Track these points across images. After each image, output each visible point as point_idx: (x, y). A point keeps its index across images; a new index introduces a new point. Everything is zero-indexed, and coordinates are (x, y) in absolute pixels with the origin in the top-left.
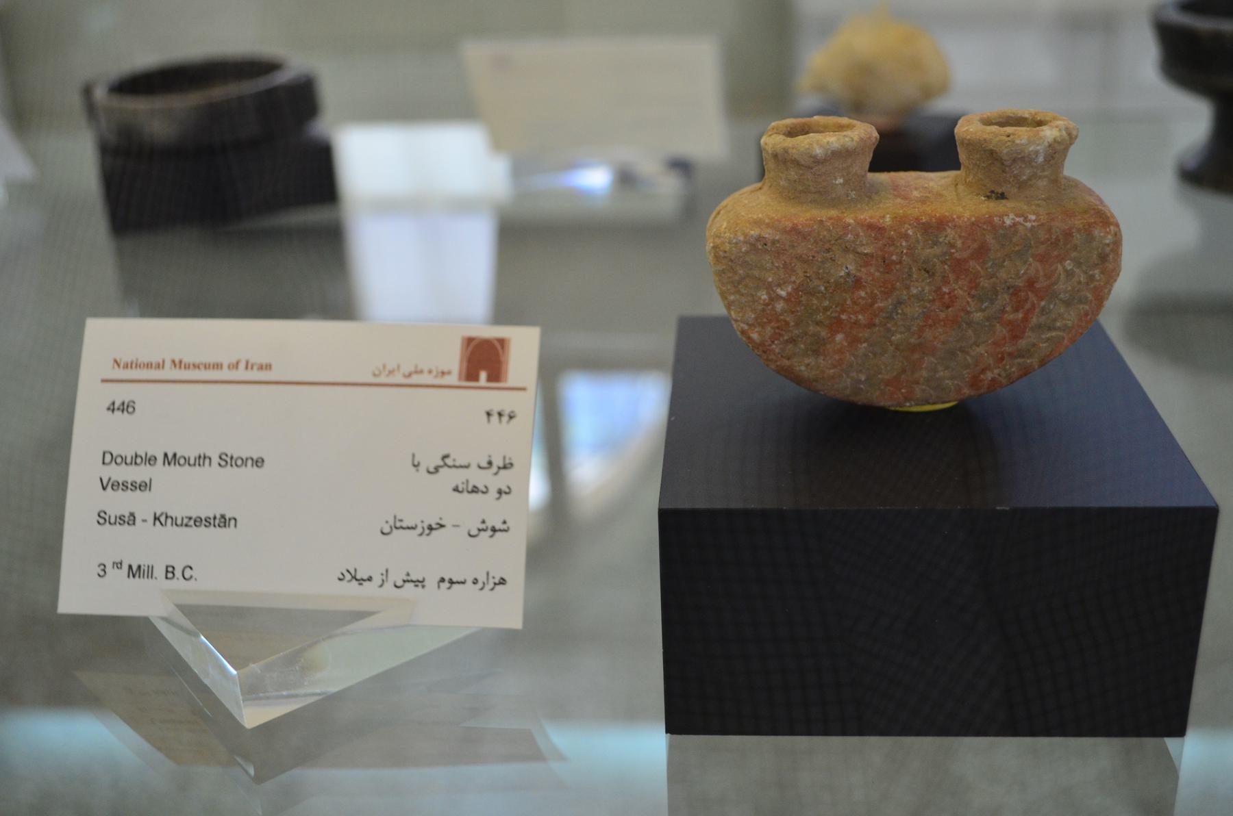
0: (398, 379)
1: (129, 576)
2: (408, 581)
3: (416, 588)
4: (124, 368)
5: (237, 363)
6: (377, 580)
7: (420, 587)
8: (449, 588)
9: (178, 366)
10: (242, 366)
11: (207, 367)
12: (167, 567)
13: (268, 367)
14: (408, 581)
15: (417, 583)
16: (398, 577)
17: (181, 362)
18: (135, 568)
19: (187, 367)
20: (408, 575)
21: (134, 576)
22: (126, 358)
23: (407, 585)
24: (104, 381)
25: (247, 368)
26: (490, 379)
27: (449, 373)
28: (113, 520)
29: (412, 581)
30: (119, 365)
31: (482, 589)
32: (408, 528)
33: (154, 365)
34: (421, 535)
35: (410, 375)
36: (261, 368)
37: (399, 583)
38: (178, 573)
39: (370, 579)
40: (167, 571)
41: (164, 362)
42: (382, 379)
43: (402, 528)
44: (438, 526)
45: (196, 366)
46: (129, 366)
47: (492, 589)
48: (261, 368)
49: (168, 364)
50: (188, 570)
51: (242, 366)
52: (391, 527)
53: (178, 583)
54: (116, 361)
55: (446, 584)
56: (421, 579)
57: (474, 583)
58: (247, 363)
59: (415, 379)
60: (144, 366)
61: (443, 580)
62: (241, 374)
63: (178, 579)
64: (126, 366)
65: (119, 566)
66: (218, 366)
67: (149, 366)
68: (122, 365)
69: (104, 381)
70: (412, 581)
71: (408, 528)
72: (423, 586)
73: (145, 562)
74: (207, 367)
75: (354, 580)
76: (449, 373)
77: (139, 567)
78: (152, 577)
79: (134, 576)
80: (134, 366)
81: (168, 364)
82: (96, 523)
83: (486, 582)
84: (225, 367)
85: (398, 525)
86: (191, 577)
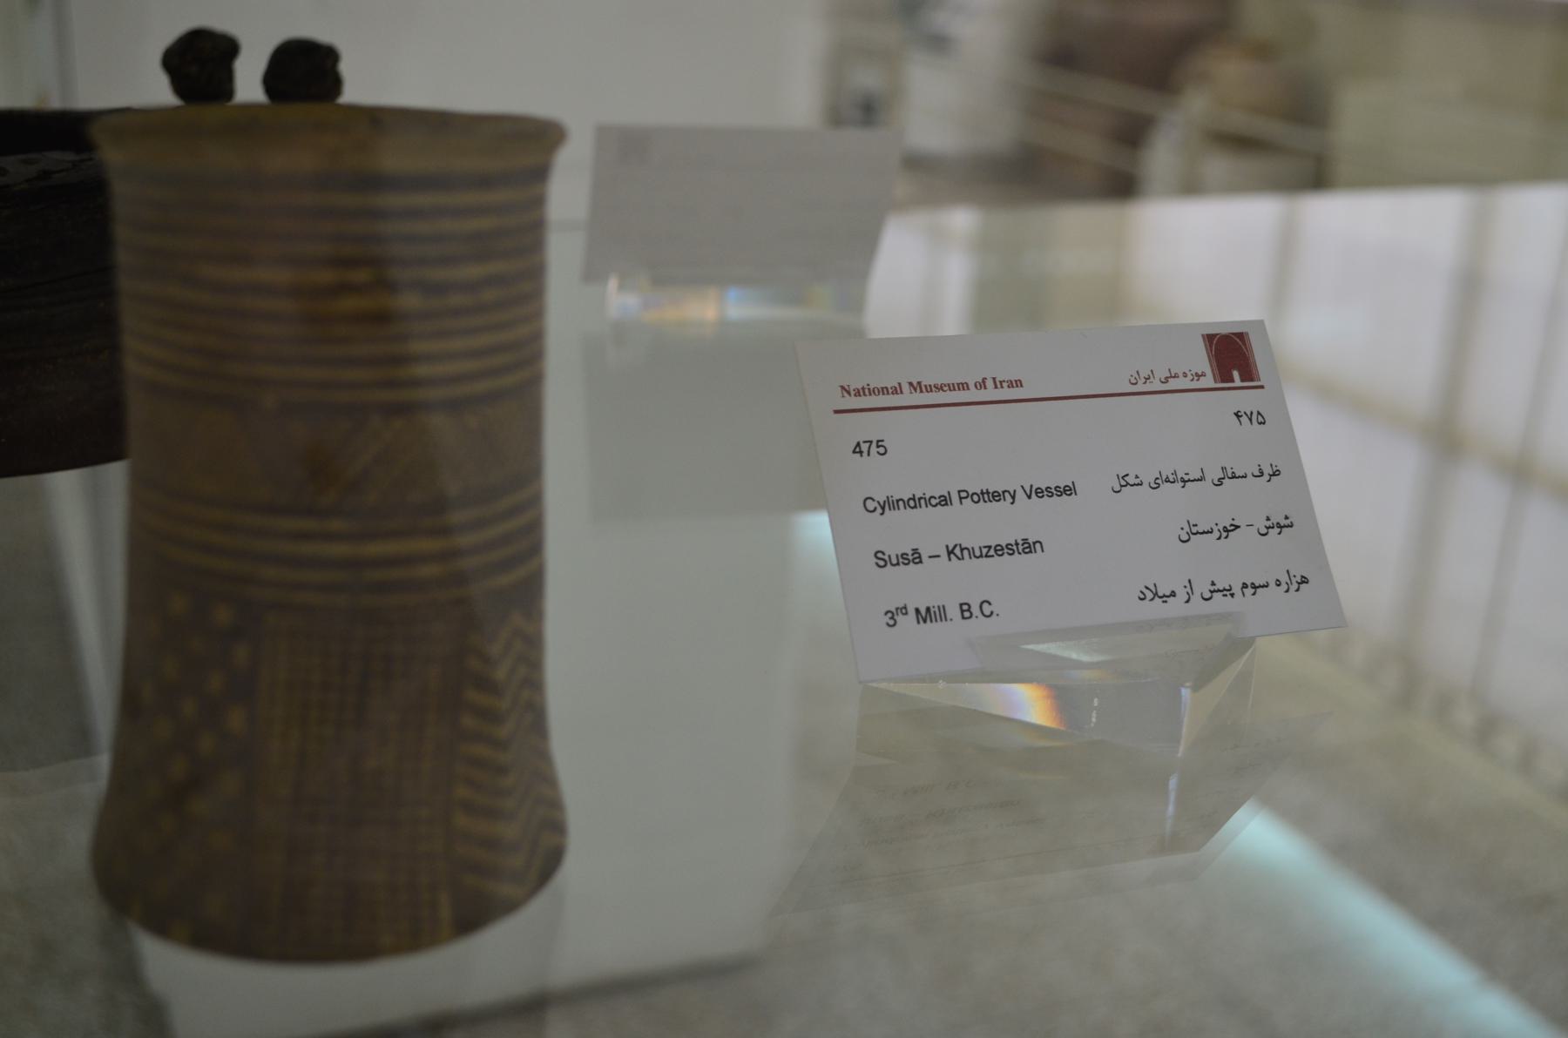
0: (1156, 385)
1: (918, 622)
2: (1215, 591)
3: (1225, 598)
4: (855, 395)
5: (984, 380)
6: (1182, 595)
7: (1229, 597)
8: (1254, 594)
9: (918, 389)
10: (990, 383)
11: (952, 387)
12: (961, 605)
13: (1018, 383)
14: (1215, 591)
15: (1225, 592)
16: (1202, 587)
17: (919, 383)
18: (923, 612)
19: (929, 389)
20: (1213, 584)
21: (925, 621)
22: (856, 384)
23: (1215, 594)
24: (837, 412)
25: (996, 387)
26: (1242, 380)
27: (1203, 375)
28: (894, 561)
29: (1219, 591)
30: (849, 393)
31: (1287, 591)
32: (1204, 533)
33: (890, 391)
34: (1219, 538)
35: (1166, 381)
36: (1011, 385)
37: (1207, 595)
38: (975, 610)
39: (1173, 594)
40: (962, 611)
41: (900, 384)
42: (1140, 388)
43: (1198, 533)
44: (1232, 528)
45: (940, 388)
46: (862, 393)
47: (1298, 590)
48: (1011, 385)
49: (906, 388)
50: (985, 606)
51: (990, 383)
52: (1188, 533)
53: (978, 625)
54: (843, 387)
55: (1249, 591)
56: (1228, 588)
57: (1279, 585)
58: (994, 379)
59: (1172, 385)
60: (879, 392)
61: (1245, 586)
62: (990, 393)
63: (977, 617)
64: (858, 394)
65: (904, 611)
66: (963, 386)
67: (884, 391)
68: (853, 393)
69: (837, 412)
70: (1219, 591)
71: (1204, 533)
72: (1232, 595)
73: (934, 603)
74: (952, 387)
75: (1156, 598)
76: (1203, 375)
77: (928, 609)
78: (946, 620)
79: (925, 621)
80: (867, 391)
81: (906, 388)
82: (876, 567)
83: (1289, 582)
84: (972, 386)
85: (1193, 532)
86: (992, 613)
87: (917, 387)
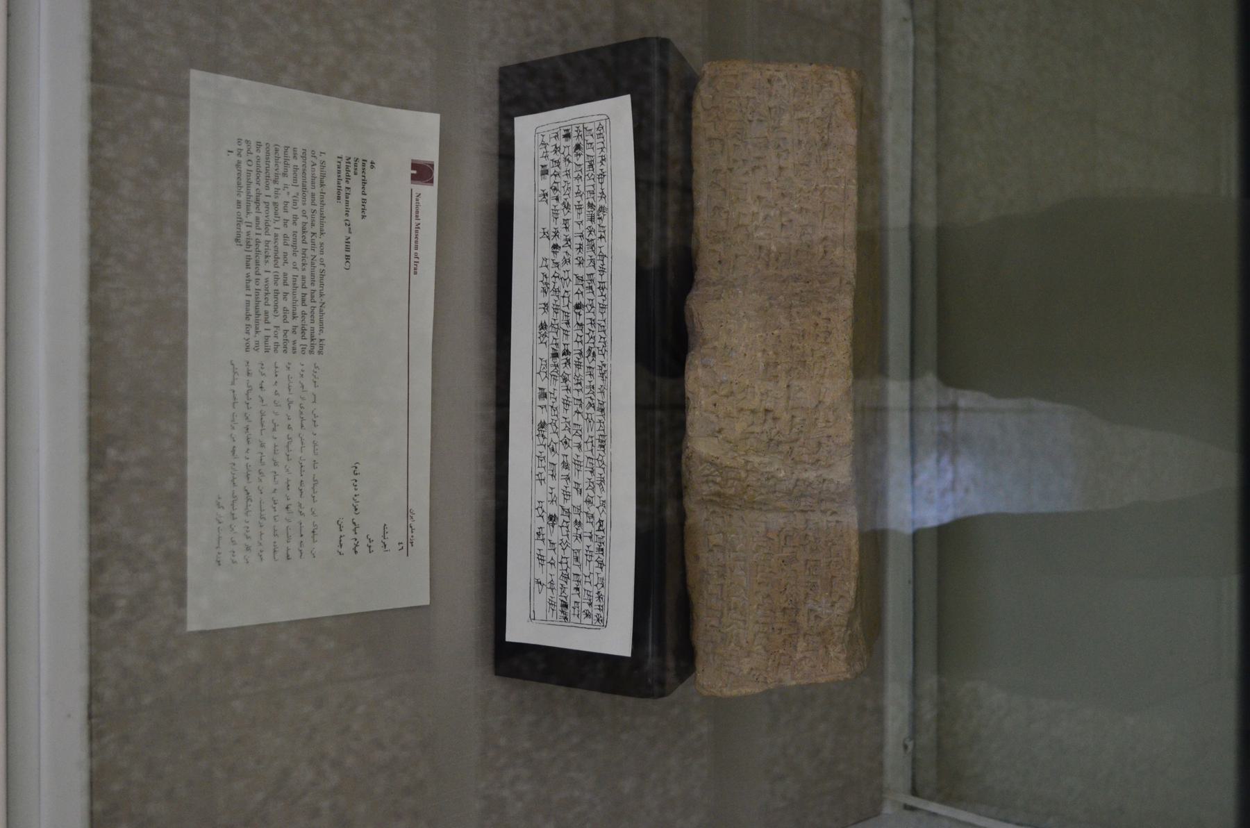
10: (416, 260)
11: (416, 242)
13: (415, 273)
17: (419, 228)
19: (417, 232)
36: (415, 269)
48: (415, 269)
51: (416, 260)
58: (418, 262)
62: (413, 259)
64: (417, 200)
66: (416, 248)
74: (416, 242)
84: (416, 251)
87: (418, 227)
